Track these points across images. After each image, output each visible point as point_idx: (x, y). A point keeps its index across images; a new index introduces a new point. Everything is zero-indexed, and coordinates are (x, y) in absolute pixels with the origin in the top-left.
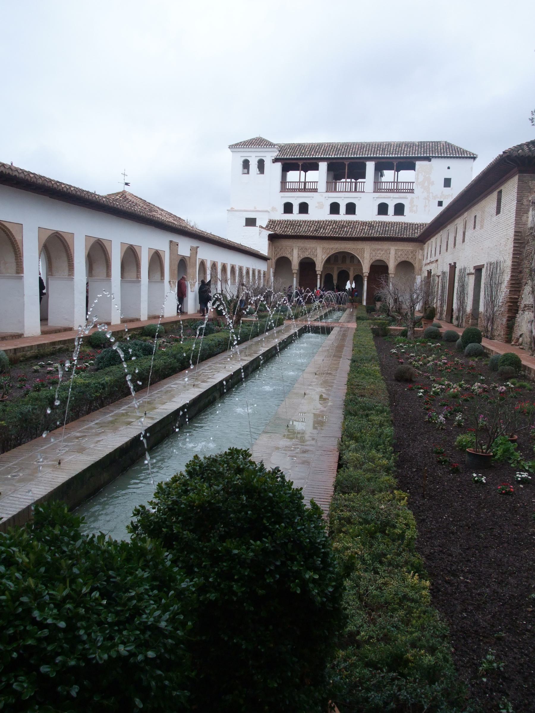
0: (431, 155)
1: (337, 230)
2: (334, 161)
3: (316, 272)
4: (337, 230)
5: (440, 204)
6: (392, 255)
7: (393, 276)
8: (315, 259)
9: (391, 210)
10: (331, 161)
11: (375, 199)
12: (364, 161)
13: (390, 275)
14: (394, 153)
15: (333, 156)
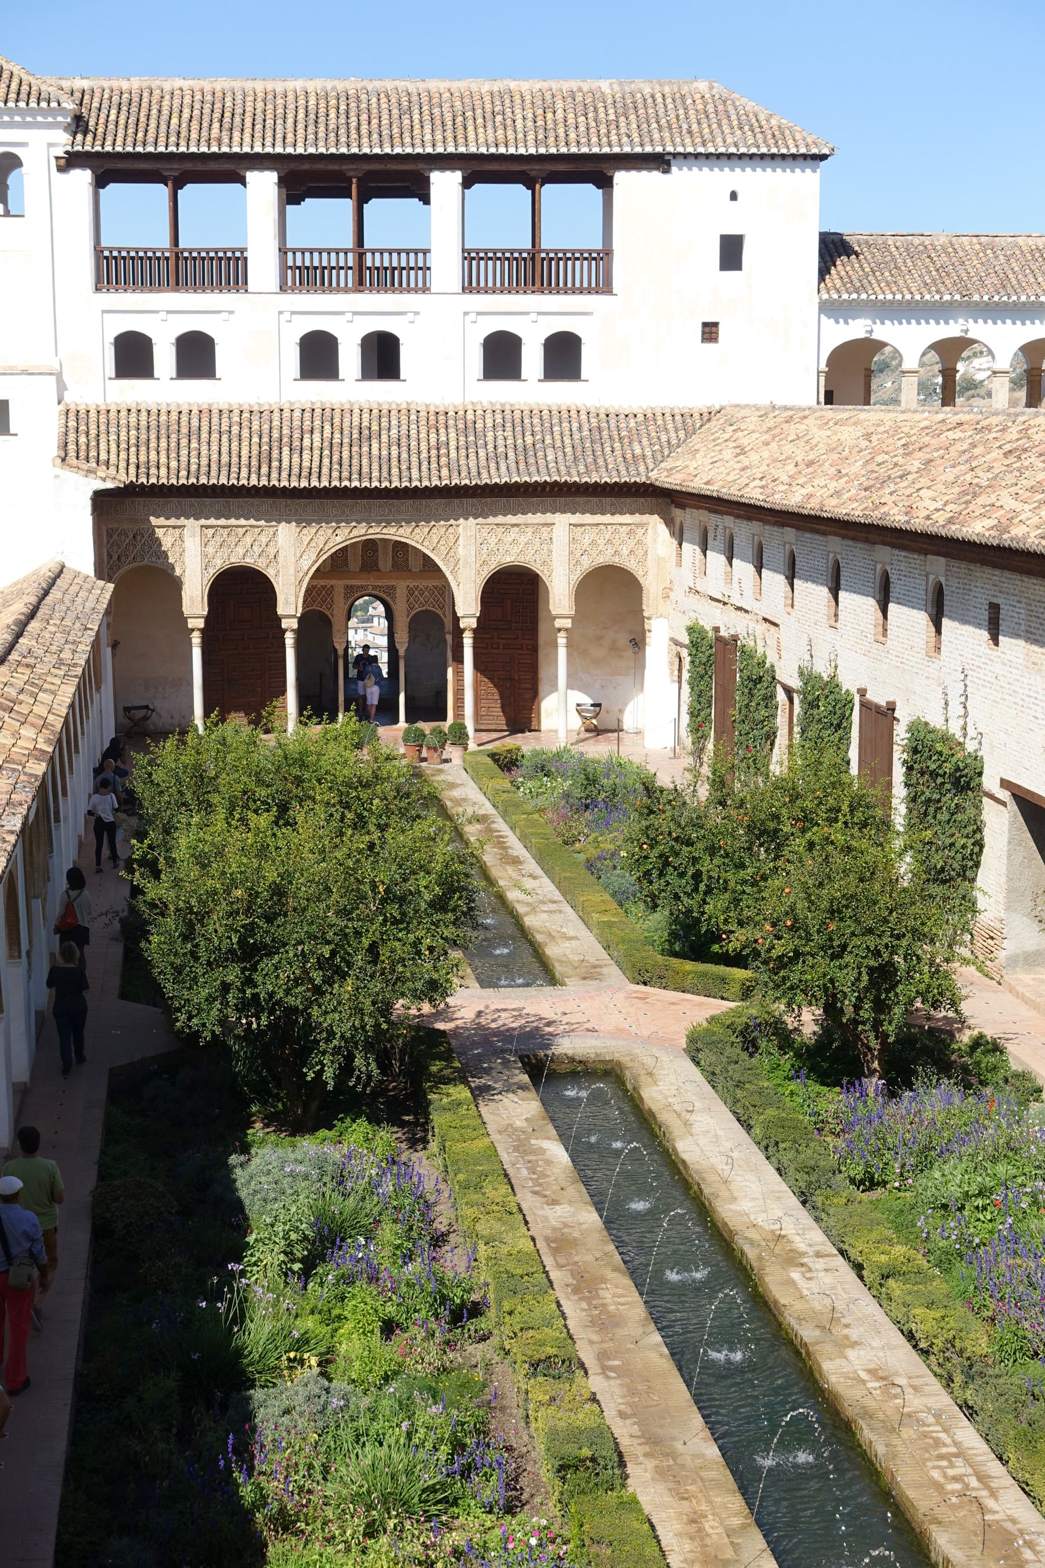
0: (670, 149)
1: (346, 454)
2: (306, 167)
3: (278, 620)
4: (346, 454)
5: (710, 331)
6: (559, 550)
7: (568, 623)
8: (270, 573)
9: (532, 359)
10: (293, 166)
11: (472, 317)
12: (421, 166)
13: (559, 623)
14: (531, 137)
15: (300, 150)
